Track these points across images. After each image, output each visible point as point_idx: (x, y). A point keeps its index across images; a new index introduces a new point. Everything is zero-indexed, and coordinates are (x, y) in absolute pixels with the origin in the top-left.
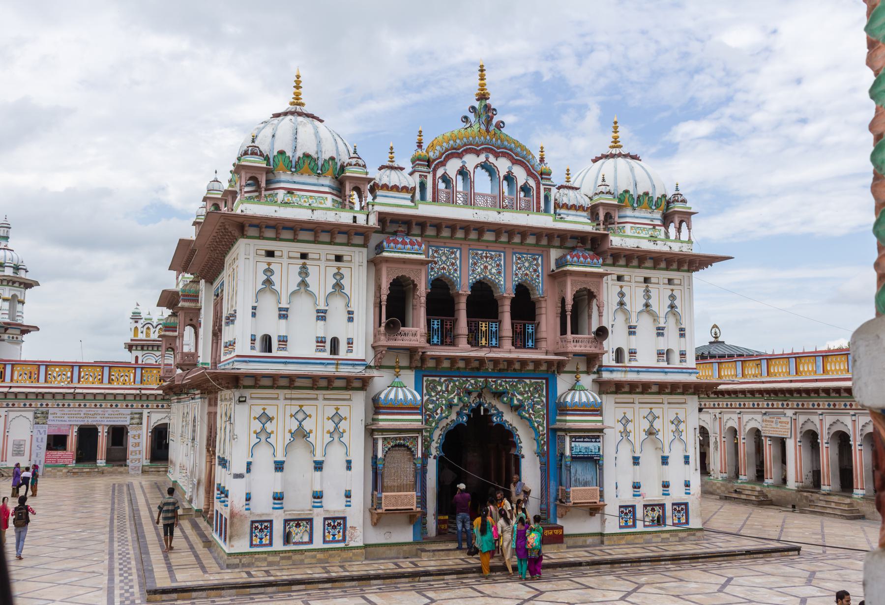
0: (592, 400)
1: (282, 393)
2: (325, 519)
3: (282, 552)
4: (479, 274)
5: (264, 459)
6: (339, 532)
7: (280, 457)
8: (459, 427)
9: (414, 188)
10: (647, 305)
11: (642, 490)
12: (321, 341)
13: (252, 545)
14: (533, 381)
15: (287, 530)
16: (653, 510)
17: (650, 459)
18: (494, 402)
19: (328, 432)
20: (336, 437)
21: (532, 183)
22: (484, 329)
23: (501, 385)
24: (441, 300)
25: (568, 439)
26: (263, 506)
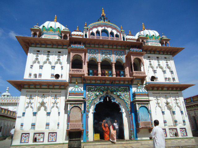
0: (144, 91)
1: (37, 90)
2: (49, 133)
3: (32, 145)
4: (104, 57)
5: (29, 112)
6: (54, 138)
7: (35, 111)
8: (100, 103)
9: (83, 35)
10: (159, 65)
11: (167, 124)
12: (52, 75)
13: (21, 142)
14: (124, 87)
15: (35, 136)
16: (173, 131)
17: (167, 112)
18: (112, 95)
19: (52, 103)
20: (55, 104)
21: (118, 34)
22: (107, 73)
23: (113, 89)
24: (92, 65)
25: (137, 105)
26: (27, 128)
